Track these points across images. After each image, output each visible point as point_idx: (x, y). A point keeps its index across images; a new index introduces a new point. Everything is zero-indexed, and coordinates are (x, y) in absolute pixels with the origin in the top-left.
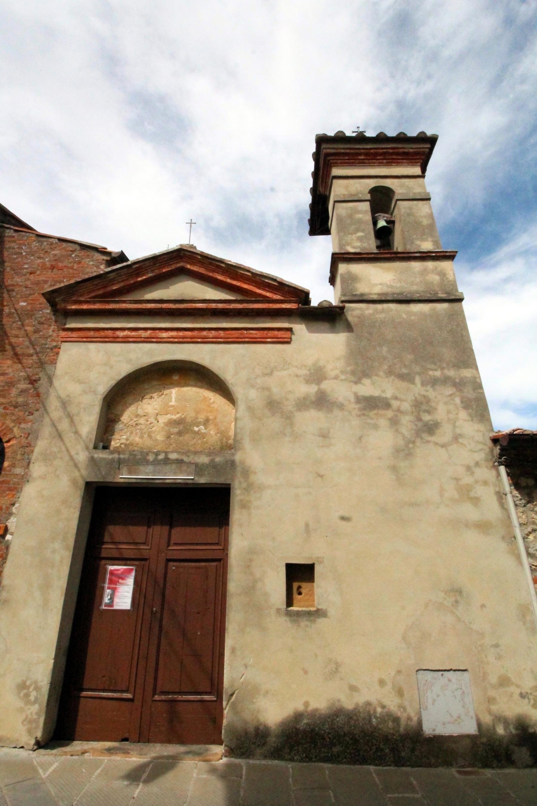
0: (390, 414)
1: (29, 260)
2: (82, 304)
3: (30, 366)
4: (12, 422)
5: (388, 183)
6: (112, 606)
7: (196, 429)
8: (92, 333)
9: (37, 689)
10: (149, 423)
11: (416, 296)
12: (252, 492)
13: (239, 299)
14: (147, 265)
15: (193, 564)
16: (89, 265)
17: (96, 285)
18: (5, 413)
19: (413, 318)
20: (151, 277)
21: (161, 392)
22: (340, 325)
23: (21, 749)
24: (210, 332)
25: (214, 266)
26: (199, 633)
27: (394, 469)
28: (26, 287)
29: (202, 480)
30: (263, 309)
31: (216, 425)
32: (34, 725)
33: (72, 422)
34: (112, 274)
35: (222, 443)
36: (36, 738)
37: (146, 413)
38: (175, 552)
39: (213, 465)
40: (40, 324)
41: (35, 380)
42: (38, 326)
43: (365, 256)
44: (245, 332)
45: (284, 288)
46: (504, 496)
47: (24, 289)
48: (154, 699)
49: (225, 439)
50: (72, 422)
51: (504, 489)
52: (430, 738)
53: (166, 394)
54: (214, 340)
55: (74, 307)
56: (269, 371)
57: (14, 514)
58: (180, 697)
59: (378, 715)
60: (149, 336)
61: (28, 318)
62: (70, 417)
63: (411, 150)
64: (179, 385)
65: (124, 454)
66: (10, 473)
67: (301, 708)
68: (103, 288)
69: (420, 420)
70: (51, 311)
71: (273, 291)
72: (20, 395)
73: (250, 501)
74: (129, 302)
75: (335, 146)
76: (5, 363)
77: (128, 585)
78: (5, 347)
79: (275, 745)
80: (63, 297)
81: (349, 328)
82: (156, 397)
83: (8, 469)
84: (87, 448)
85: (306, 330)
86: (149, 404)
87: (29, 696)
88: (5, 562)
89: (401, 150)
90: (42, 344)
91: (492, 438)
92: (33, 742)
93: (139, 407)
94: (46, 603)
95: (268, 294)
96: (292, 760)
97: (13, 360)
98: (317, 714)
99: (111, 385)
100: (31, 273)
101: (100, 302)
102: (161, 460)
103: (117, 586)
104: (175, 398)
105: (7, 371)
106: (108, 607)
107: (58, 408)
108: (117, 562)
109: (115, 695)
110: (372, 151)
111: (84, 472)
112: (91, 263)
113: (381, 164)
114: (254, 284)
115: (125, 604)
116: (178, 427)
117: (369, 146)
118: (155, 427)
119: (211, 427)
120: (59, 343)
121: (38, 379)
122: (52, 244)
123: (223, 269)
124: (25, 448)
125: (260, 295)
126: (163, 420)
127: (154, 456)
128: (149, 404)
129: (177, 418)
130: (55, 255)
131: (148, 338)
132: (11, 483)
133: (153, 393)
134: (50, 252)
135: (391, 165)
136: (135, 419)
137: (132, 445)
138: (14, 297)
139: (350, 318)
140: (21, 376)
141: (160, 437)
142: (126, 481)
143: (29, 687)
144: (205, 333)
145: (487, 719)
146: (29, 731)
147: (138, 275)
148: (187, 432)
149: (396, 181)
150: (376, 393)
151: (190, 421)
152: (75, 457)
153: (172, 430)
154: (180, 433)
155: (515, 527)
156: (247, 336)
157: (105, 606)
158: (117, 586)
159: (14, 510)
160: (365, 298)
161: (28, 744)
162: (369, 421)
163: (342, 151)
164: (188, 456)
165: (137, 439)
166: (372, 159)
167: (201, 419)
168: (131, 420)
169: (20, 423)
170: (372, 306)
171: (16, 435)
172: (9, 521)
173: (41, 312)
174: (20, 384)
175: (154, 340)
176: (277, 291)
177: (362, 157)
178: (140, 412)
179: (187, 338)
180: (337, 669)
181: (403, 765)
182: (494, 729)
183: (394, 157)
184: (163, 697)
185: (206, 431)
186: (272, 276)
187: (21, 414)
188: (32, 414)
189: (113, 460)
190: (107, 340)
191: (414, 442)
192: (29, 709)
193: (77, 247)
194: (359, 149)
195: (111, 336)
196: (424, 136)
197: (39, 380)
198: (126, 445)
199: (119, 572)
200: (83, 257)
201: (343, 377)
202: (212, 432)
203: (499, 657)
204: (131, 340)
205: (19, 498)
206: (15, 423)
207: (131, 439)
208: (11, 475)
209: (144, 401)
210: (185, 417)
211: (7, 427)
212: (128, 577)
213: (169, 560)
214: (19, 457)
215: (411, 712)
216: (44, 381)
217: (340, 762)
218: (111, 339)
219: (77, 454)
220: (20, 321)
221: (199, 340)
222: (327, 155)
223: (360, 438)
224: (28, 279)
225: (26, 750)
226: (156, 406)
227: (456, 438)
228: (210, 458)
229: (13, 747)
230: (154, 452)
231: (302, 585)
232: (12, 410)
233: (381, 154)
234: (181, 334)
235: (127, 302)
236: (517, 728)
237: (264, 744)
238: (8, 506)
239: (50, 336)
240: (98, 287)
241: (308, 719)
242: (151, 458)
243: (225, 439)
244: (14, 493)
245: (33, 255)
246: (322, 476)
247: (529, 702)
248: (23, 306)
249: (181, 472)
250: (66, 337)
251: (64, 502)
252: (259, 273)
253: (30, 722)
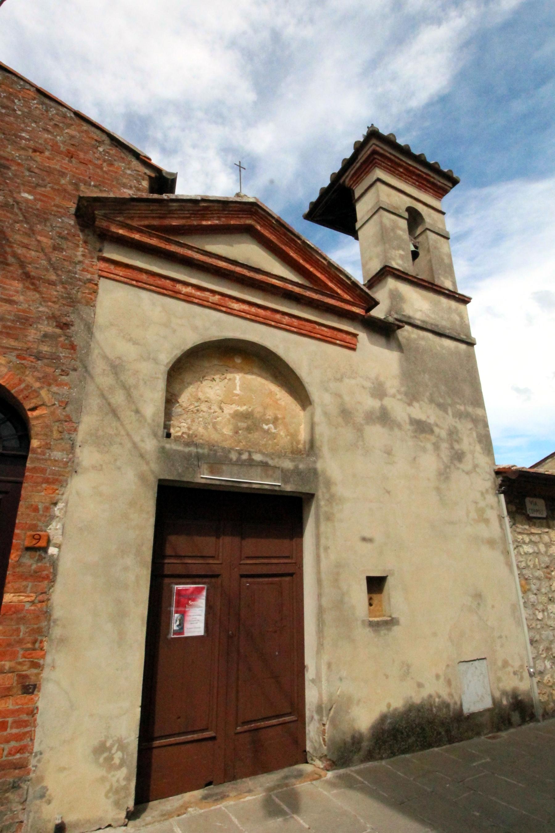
0: (433, 439)
1: (29, 127)
2: (133, 231)
3: (56, 300)
4: (36, 381)
5: (420, 207)
6: (182, 633)
7: (266, 427)
8: (144, 277)
9: (122, 747)
10: (212, 411)
11: (447, 332)
12: (334, 504)
13: (300, 282)
14: (216, 208)
15: (266, 579)
16: (126, 173)
17: (152, 210)
18: (20, 363)
19: (444, 351)
20: (217, 225)
21: (224, 375)
22: (393, 344)
23: (108, 829)
24: (283, 316)
25: (287, 239)
26: (277, 653)
27: (438, 489)
28: (29, 170)
29: (289, 488)
30: (335, 306)
31: (286, 425)
32: (123, 794)
33: (129, 396)
34: (175, 204)
35: (292, 447)
36: (128, 808)
37: (208, 398)
38: (248, 567)
39: (297, 472)
40: (62, 238)
41: (65, 324)
42: (58, 241)
43: (410, 278)
44: (317, 327)
45: (357, 290)
46: (502, 518)
47: (27, 173)
48: (237, 731)
49: (295, 443)
50: (129, 396)
51: (503, 514)
52: (468, 716)
53: (230, 379)
54: (288, 327)
55: (121, 232)
56: (339, 376)
57: (58, 517)
58: (262, 724)
59: (437, 704)
60: (217, 302)
61: (40, 223)
62: (125, 388)
63: (439, 183)
64: (240, 370)
65: (201, 448)
66: (43, 457)
67: (384, 709)
68: (160, 218)
69: (452, 448)
70: (75, 223)
71: (345, 290)
72: (43, 342)
73: (333, 514)
74: (196, 250)
75: (386, 148)
76: (11, 285)
77: (200, 607)
78: (6, 259)
79: (368, 748)
80: (107, 212)
81: (400, 348)
82: (218, 380)
83: (39, 450)
84: (155, 435)
85: (367, 340)
86: (210, 387)
87: (112, 759)
88: (52, 586)
89: (432, 180)
90: (69, 271)
91: (496, 471)
92: (123, 814)
93: (199, 389)
94: (121, 637)
95: (339, 291)
96: (382, 759)
97: (24, 284)
98: (396, 712)
99: (175, 356)
100: (35, 151)
101: (158, 237)
102: (245, 461)
103: (187, 609)
104: (240, 386)
105: (15, 298)
106: (177, 635)
107: (106, 372)
108: (183, 580)
109: (196, 736)
110: (411, 168)
111: (154, 466)
112: (129, 172)
113: (413, 184)
114: (327, 275)
115: (198, 630)
116: (246, 422)
117: (410, 162)
118: (220, 418)
119: (281, 428)
120: (96, 276)
121: (71, 323)
122: (65, 117)
123: (298, 246)
124: (63, 422)
125: (331, 289)
126: (229, 409)
127: (237, 455)
128: (210, 387)
129: (244, 410)
130: (72, 137)
131: (217, 304)
132: (48, 471)
133: (214, 375)
134: (64, 130)
135: (421, 190)
136: (196, 404)
137: (196, 436)
138: (10, 178)
139: (400, 338)
140: (40, 311)
141: (227, 431)
142: (208, 482)
143: (110, 749)
144: (278, 316)
145: (497, 694)
146: (117, 804)
147: (204, 218)
148: (257, 429)
149: (425, 208)
150: (423, 417)
151: (258, 416)
152: (141, 445)
153: (239, 424)
154: (249, 429)
155: (509, 543)
156: (320, 332)
157: (174, 634)
158: (187, 609)
159: (57, 511)
160: (412, 321)
161: (116, 820)
162: (420, 443)
163: (388, 155)
164: (272, 459)
165: (201, 430)
166: (409, 177)
167: (269, 416)
168: (191, 404)
169: (49, 385)
170: (416, 331)
171: (46, 399)
172: (50, 527)
173: (60, 220)
174: (41, 324)
175: (224, 309)
176: (348, 291)
177: (401, 170)
178: (200, 395)
179: (259, 317)
180: (408, 670)
181: (453, 742)
182: (501, 700)
183: (425, 183)
184: (246, 727)
185: (275, 431)
186: (347, 273)
187: (49, 370)
188: (68, 375)
189: (190, 454)
190: (165, 292)
191: (449, 467)
192: (113, 776)
193: (107, 141)
194: (401, 160)
195: (170, 289)
196: (451, 175)
197: (72, 325)
198: (188, 435)
199: (188, 592)
200: (116, 158)
201: (399, 397)
202: (282, 433)
203: (502, 646)
204: (196, 301)
205: (63, 494)
206: (40, 382)
207: (194, 428)
208: (46, 460)
209: (205, 383)
210: (252, 411)
211: (28, 386)
212: (198, 598)
213: (242, 576)
214: (56, 435)
215: (457, 698)
216: (78, 328)
217: (413, 751)
218: (170, 293)
219: (143, 441)
220: (28, 223)
221: (273, 323)
222: (374, 152)
223: (415, 459)
224: (32, 159)
225: (115, 828)
226: (218, 391)
227: (476, 466)
228: (294, 464)
229: (95, 828)
230: (237, 450)
231: (373, 597)
232: (32, 362)
233: (418, 176)
234: (253, 310)
235: (194, 249)
236: (512, 698)
237: (359, 750)
238: (47, 505)
239: (80, 262)
240: (154, 215)
241: (391, 719)
242: (234, 456)
243: (295, 443)
244: (55, 487)
245: (35, 122)
246: (389, 492)
247: (518, 677)
248: (27, 200)
249: (268, 477)
250: (106, 270)
251: (132, 504)
252: (336, 265)
253: (117, 792)
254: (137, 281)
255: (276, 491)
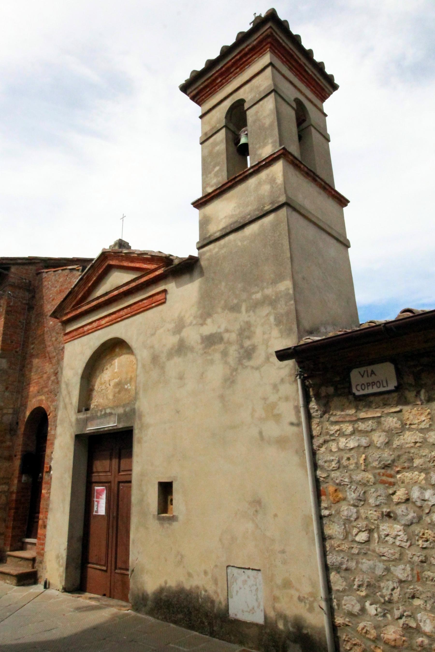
0: (221, 347)
11: (248, 218)
27: (222, 397)
29: (120, 426)
33: (70, 396)
43: (213, 195)
52: (232, 620)
67: (163, 584)
110: (224, 69)
113: (236, 75)
126: (112, 383)
163: (202, 86)
170: (217, 244)
177: (219, 80)
178: (103, 381)
181: (214, 637)
182: (276, 623)
183: (245, 59)
213: (119, 482)
215: (222, 598)
221: (119, 319)
233: (232, 66)
246: (178, 412)
254: (78, 335)
255: (114, 429)
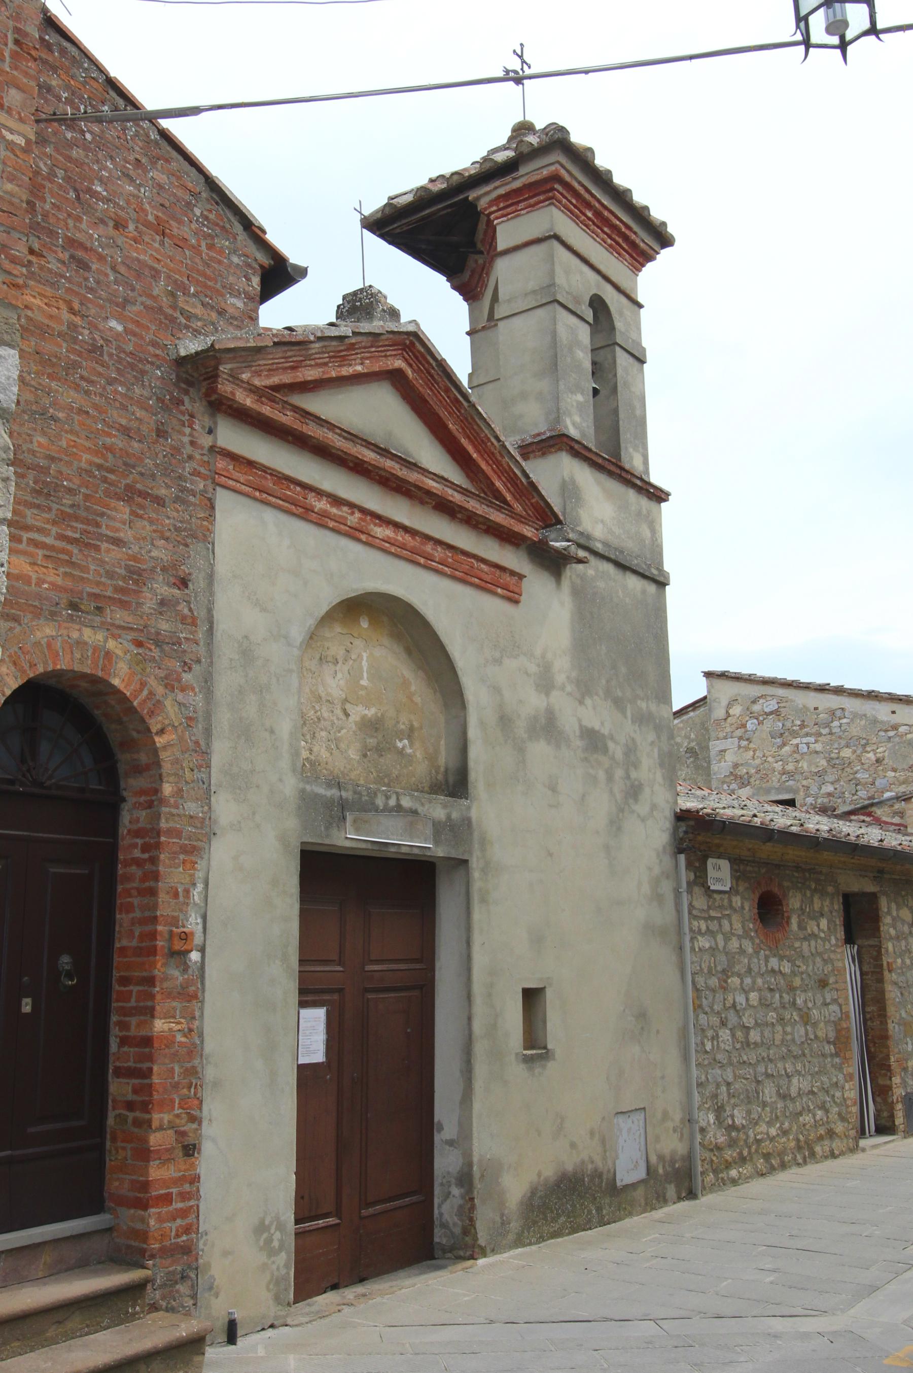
9: (281, 1227)
11: (634, 563)
45: (533, 497)
59: (589, 1172)
63: (642, 245)
69: (628, 777)
80: (235, 365)
87: (272, 1241)
89: (633, 237)
96: (530, 1244)
102: (393, 807)
144: (429, 548)
154: (379, 750)
165: (324, 754)
177: (590, 214)
183: (620, 241)
192: (274, 1262)
221: (422, 561)
233: (614, 227)
250: (224, 473)
